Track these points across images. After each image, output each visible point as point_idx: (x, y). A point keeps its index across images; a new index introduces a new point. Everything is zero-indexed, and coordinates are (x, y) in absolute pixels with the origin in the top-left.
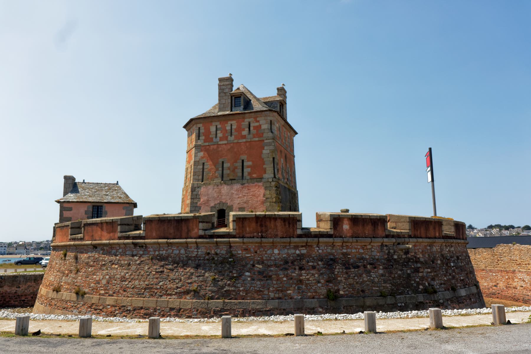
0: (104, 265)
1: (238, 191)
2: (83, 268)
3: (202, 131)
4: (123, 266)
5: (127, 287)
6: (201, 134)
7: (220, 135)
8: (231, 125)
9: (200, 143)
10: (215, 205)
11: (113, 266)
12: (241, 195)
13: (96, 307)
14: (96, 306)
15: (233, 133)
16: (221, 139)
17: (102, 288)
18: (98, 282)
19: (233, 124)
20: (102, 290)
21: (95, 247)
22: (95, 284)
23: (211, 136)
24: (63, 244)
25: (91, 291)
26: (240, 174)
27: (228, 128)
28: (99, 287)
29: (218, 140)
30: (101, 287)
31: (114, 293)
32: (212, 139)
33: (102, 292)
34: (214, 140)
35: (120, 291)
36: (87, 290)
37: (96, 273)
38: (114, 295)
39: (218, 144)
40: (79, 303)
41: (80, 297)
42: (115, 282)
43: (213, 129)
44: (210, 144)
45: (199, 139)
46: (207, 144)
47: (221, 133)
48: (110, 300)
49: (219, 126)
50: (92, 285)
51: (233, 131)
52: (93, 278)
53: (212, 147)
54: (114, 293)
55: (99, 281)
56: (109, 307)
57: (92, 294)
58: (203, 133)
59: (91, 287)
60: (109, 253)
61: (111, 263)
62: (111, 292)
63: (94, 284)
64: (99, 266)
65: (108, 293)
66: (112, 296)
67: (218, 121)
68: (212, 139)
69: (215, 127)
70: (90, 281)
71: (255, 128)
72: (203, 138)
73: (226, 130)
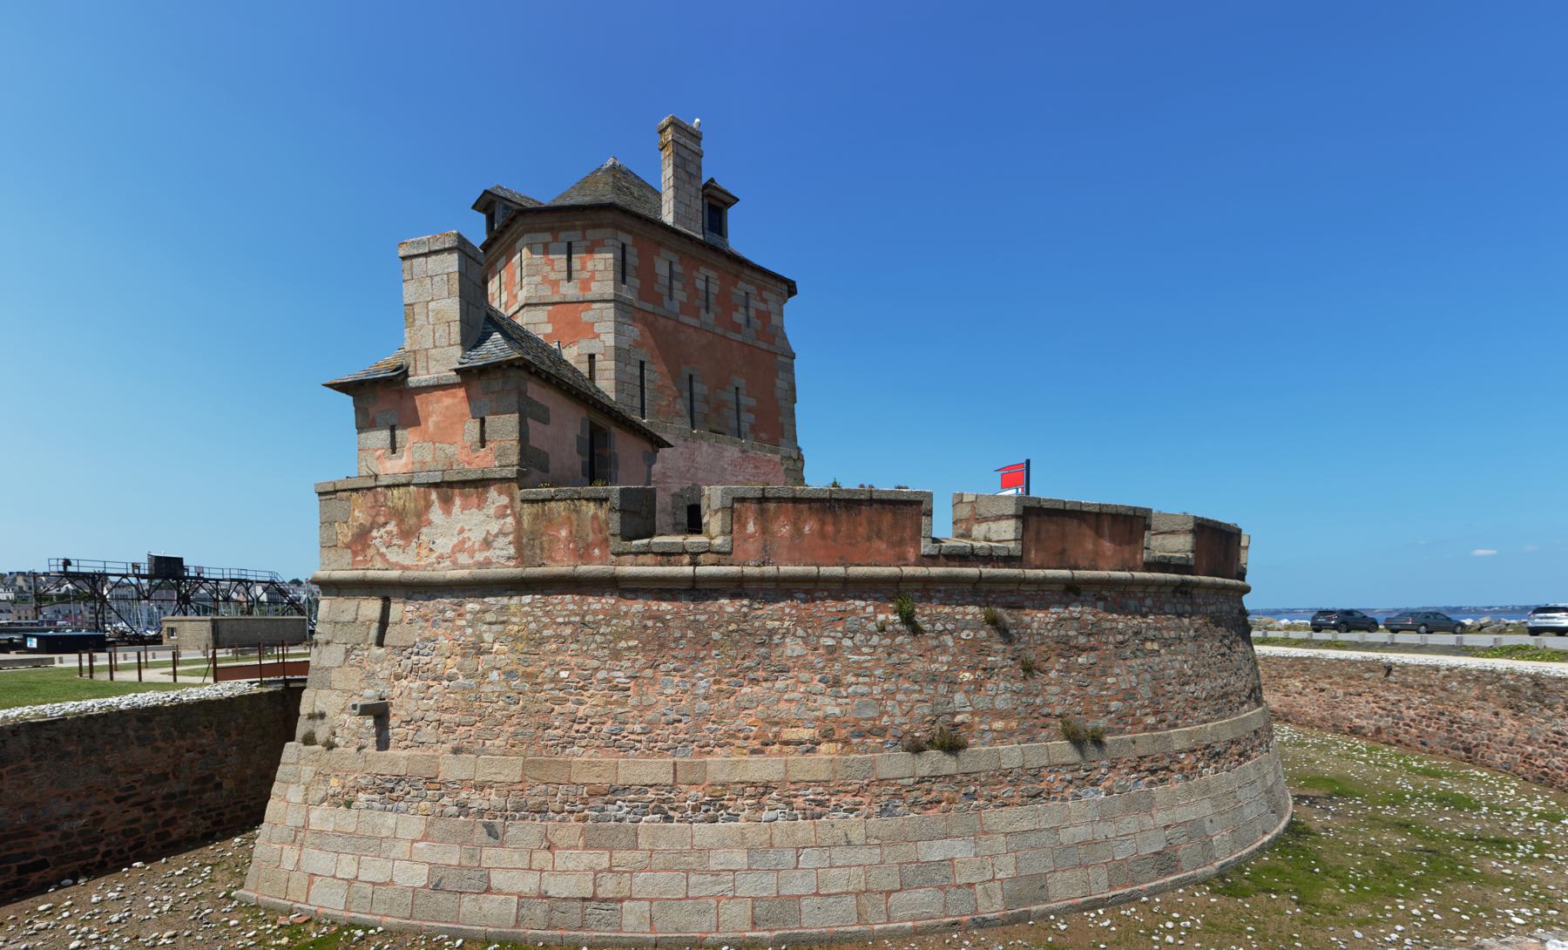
0: (1122, 643)
1: (735, 466)
2: (1053, 659)
3: (632, 260)
4: (1170, 646)
5: (1196, 698)
6: (629, 269)
7: (680, 295)
8: (707, 278)
9: (628, 295)
10: (682, 490)
11: (1149, 645)
12: (741, 478)
13: (1155, 765)
14: (1152, 761)
15: (711, 306)
16: (686, 308)
17: (1148, 710)
18: (1129, 695)
19: (710, 280)
20: (1147, 714)
21: (1072, 591)
22: (1124, 700)
23: (657, 288)
24: (800, 570)
25: (1117, 723)
26: (734, 424)
27: (700, 285)
28: (1137, 708)
29: (678, 311)
30: (1143, 707)
31: (1177, 718)
32: (660, 296)
33: (1151, 720)
34: (666, 299)
35: (1187, 709)
36: (1102, 723)
37: (1109, 671)
38: (1179, 722)
39: (677, 321)
40: (1095, 765)
41: (1091, 750)
42: (1170, 688)
43: (662, 268)
44: (656, 311)
45: (624, 282)
46: (649, 307)
47: (684, 290)
48: (1178, 738)
49: (677, 268)
50: (1114, 705)
51: (711, 297)
52: (1106, 684)
53: (661, 320)
54: (1177, 718)
55: (1132, 691)
56: (1182, 756)
57: (1121, 731)
58: (635, 268)
59: (1111, 713)
60: (1123, 610)
61: (1140, 637)
62: (1170, 717)
63: (1119, 700)
64: (1111, 647)
65: (1164, 721)
66: (1176, 726)
67: (677, 252)
68: (660, 296)
69: (667, 264)
70: (1102, 696)
71: (759, 313)
72: (633, 281)
73: (696, 290)
